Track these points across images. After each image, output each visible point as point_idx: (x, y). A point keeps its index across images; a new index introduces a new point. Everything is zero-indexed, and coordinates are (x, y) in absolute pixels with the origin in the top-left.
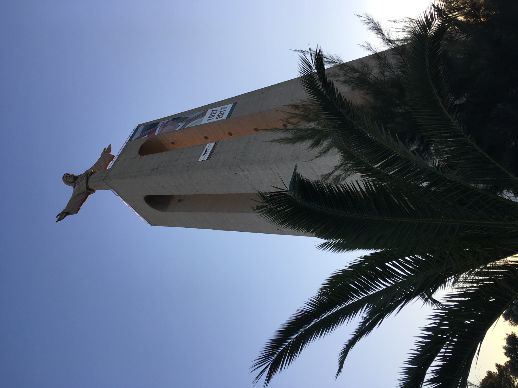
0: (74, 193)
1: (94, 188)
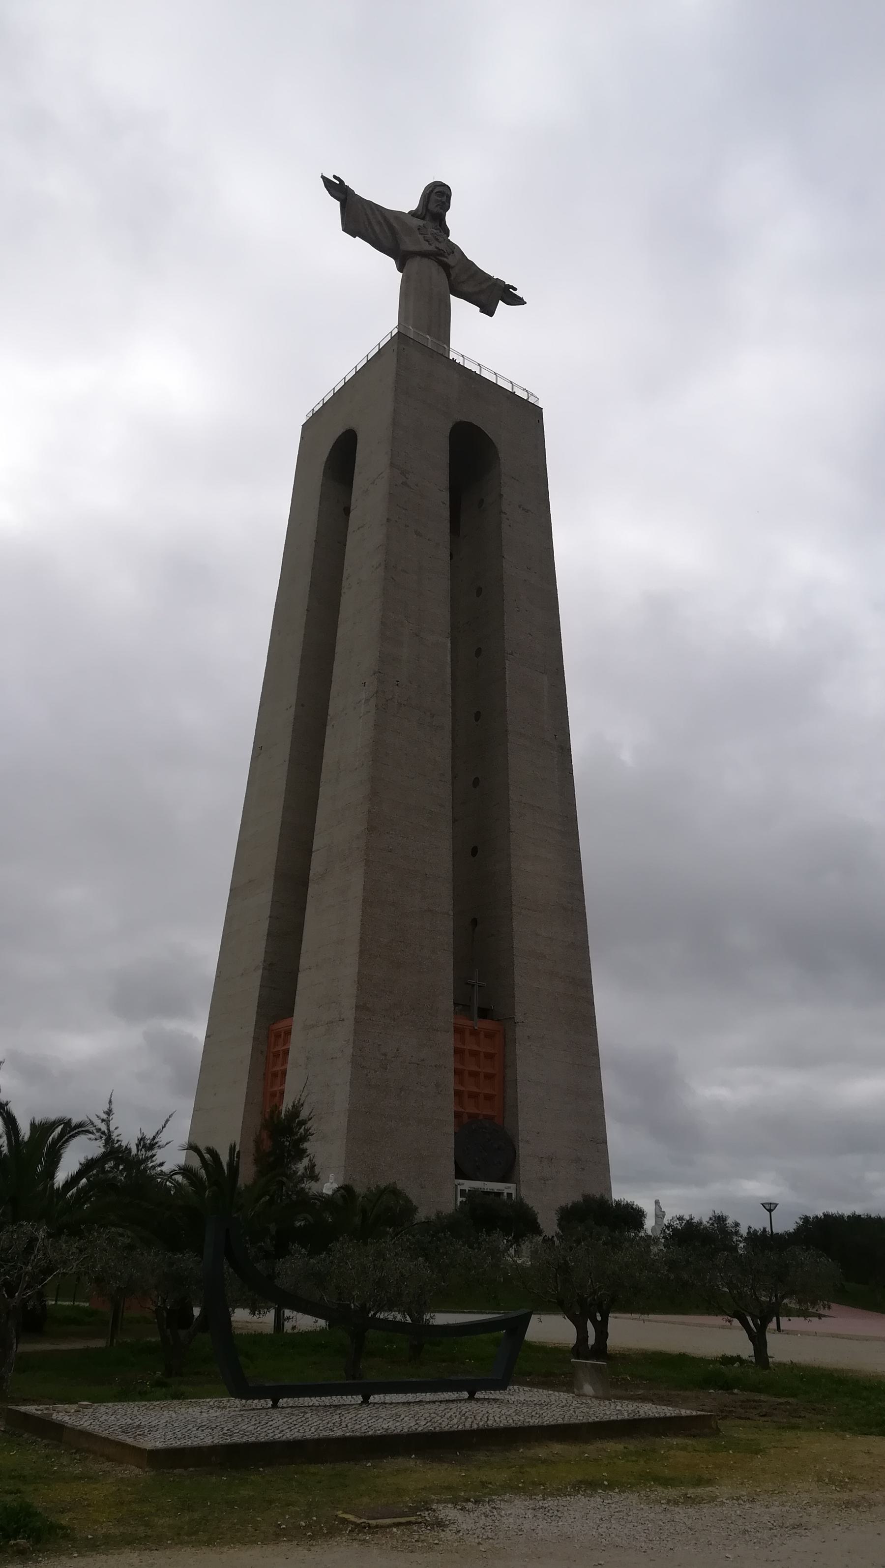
0: (398, 215)
1: (405, 270)
